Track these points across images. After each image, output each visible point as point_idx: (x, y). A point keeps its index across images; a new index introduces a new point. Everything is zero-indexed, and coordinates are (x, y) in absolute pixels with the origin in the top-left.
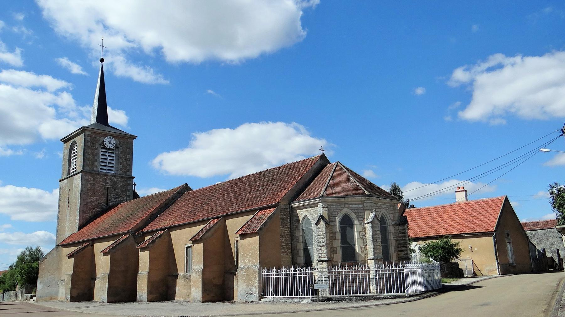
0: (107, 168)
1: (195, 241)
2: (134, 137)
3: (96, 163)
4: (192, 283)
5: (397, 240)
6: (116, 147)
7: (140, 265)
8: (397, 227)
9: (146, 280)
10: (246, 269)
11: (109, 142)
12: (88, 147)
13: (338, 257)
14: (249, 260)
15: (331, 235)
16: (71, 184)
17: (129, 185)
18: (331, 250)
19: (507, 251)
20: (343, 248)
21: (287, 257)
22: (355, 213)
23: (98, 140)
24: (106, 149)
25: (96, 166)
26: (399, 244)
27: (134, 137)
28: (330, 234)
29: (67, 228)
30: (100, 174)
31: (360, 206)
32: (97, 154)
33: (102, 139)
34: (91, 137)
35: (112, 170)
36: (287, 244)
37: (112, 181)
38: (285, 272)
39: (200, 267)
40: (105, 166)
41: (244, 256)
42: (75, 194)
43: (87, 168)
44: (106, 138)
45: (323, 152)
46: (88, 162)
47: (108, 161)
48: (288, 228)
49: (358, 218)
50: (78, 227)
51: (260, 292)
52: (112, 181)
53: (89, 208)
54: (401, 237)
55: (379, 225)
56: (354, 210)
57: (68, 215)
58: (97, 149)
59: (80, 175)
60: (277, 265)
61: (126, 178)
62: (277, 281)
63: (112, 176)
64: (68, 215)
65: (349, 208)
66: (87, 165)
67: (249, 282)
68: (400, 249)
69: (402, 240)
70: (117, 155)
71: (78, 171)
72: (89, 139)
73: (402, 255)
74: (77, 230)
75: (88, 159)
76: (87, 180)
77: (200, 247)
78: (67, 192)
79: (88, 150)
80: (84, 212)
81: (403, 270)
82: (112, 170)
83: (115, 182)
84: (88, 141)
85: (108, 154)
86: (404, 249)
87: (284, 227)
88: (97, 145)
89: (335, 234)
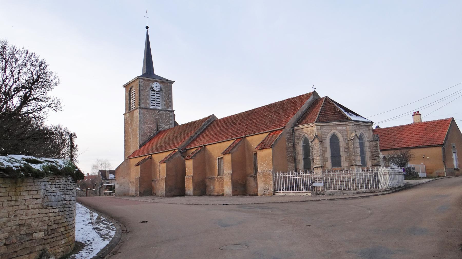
0: (155, 105)
1: (225, 153)
2: (173, 82)
3: (148, 101)
4: (225, 183)
5: (371, 152)
6: (161, 90)
7: (186, 171)
8: (372, 143)
9: (192, 181)
10: (263, 173)
11: (156, 86)
12: (142, 90)
13: (329, 164)
14: (265, 167)
15: (324, 149)
16: (132, 116)
17: (171, 116)
18: (324, 160)
19: (453, 159)
20: (332, 158)
21: (292, 165)
22: (341, 133)
23: (148, 86)
24: (154, 91)
25: (148, 104)
26: (373, 155)
27: (173, 82)
28: (323, 148)
29: (131, 147)
30: (151, 109)
31: (344, 128)
32: (148, 95)
33: (151, 84)
34: (144, 83)
36: (291, 156)
38: (291, 175)
39: (230, 172)
41: (261, 164)
42: (136, 123)
43: (143, 106)
45: (315, 90)
46: (143, 101)
47: (156, 100)
48: (291, 144)
49: (343, 137)
50: (139, 146)
51: (274, 189)
53: (146, 133)
54: (374, 149)
55: (358, 141)
56: (339, 131)
57: (131, 138)
59: (138, 110)
60: (285, 170)
61: (169, 111)
62: (285, 182)
63: (159, 110)
64: (131, 138)
65: (336, 129)
66: (143, 103)
67: (265, 182)
68: (373, 158)
69: (375, 152)
70: (162, 95)
71: (137, 107)
72: (142, 84)
73: (375, 162)
74: (139, 148)
75: (143, 99)
76: (143, 114)
77: (228, 158)
78: (130, 122)
79: (142, 93)
80: (142, 135)
81: (377, 173)
83: (162, 115)
85: (156, 95)
86: (377, 158)
87: (288, 144)
88: (148, 89)
89: (326, 148)
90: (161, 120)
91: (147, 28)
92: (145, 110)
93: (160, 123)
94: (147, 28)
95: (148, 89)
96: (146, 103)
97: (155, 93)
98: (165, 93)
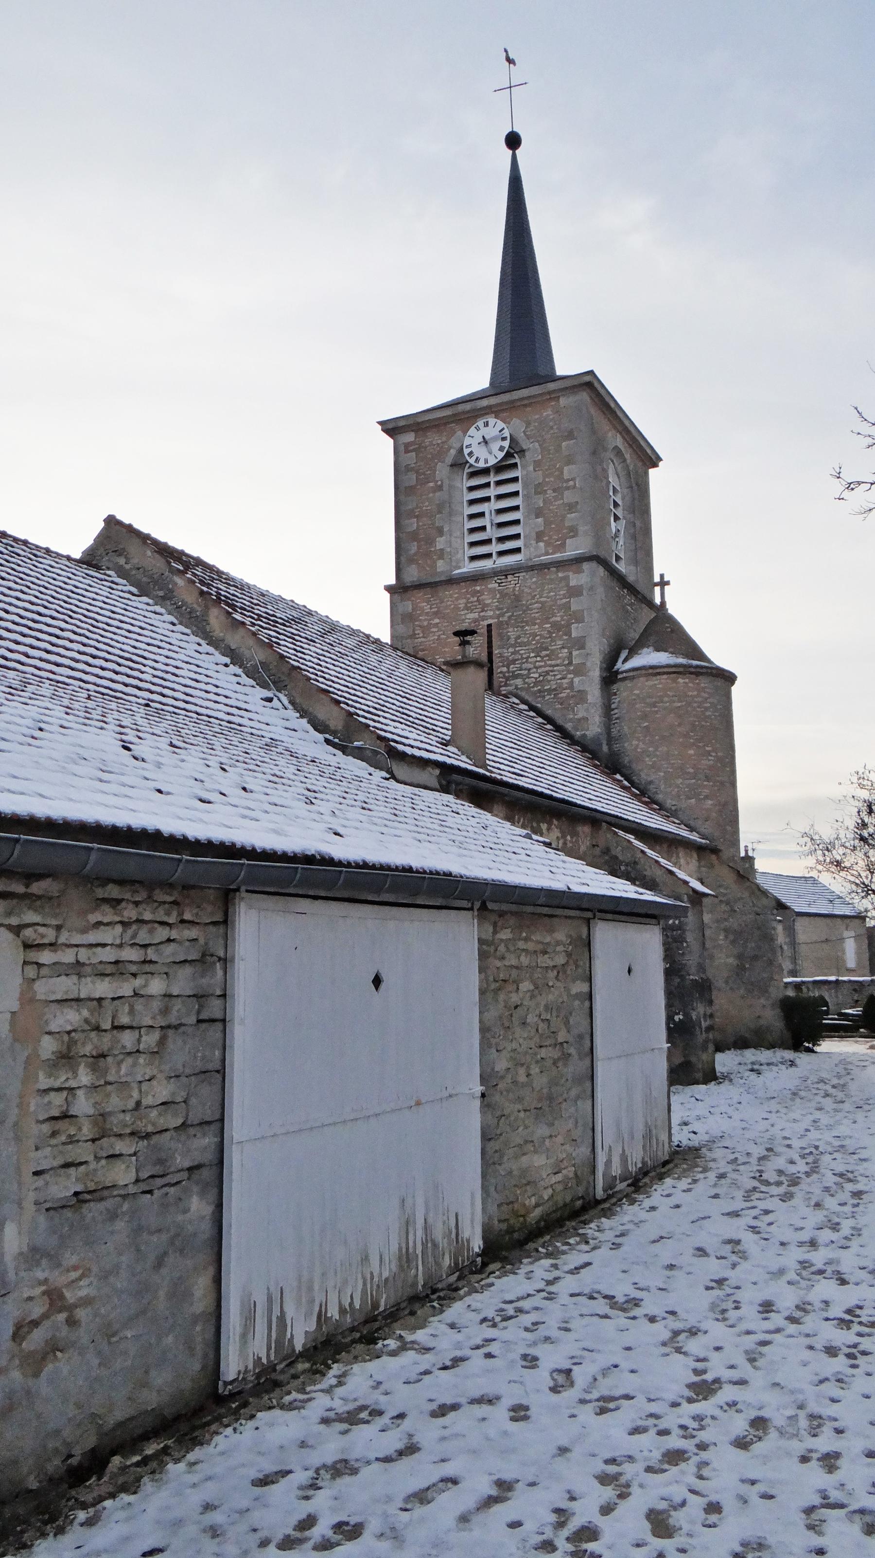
3: (440, 543)
24: (485, 471)
35: (518, 550)
37: (503, 595)
40: (488, 542)
44: (470, 432)
46: (413, 548)
47: (485, 522)
52: (503, 595)
58: (440, 488)
66: (411, 561)
72: (410, 458)
82: (518, 550)
83: (518, 598)
84: (408, 469)
88: (442, 471)
90: (512, 633)
91: (513, 141)
92: (419, 594)
93: (508, 653)
94: (513, 141)
95: (442, 471)
96: (427, 555)
97: (492, 478)
98: (537, 464)
